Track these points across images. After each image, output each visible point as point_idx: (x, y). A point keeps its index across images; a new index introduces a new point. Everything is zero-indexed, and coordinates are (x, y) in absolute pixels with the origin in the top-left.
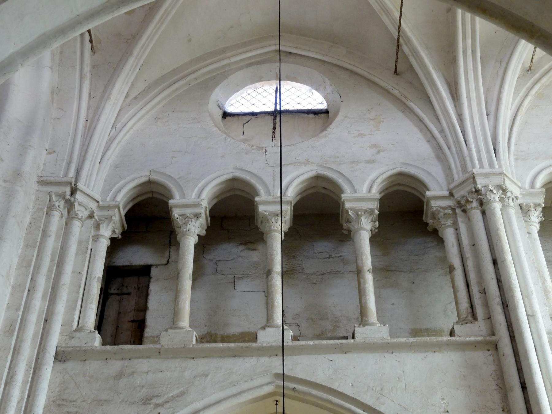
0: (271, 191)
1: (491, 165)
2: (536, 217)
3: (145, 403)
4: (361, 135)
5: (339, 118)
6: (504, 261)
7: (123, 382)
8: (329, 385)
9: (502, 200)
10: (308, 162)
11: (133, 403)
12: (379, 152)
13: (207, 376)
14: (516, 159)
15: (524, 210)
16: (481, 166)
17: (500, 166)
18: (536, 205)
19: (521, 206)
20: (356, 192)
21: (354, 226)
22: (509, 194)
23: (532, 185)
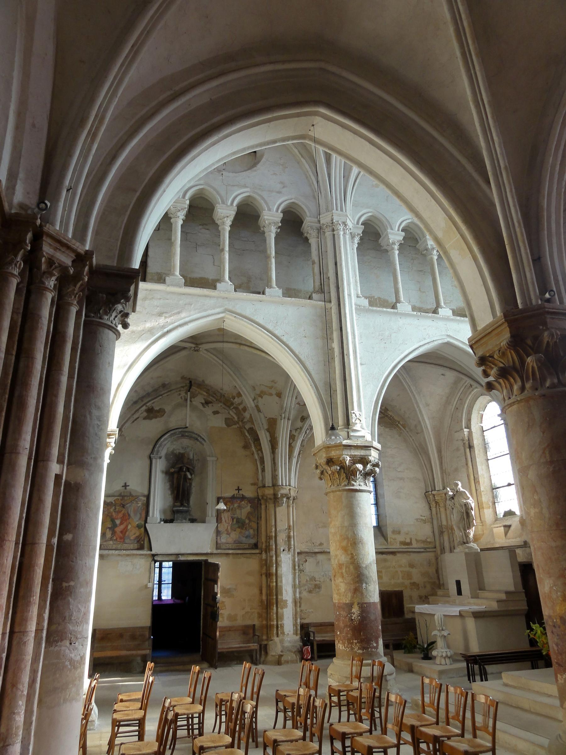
0: (225, 201)
1: (342, 210)
2: (357, 240)
3: (159, 316)
4: (275, 174)
5: (264, 160)
6: (341, 265)
7: (147, 302)
8: (252, 318)
9: (344, 229)
10: (245, 186)
11: (153, 315)
12: (284, 187)
13: (191, 305)
14: (353, 206)
15: (352, 236)
16: (337, 210)
17: (346, 211)
18: (358, 234)
19: (351, 233)
20: (270, 211)
21: (266, 230)
22: (348, 227)
23: (358, 223)
